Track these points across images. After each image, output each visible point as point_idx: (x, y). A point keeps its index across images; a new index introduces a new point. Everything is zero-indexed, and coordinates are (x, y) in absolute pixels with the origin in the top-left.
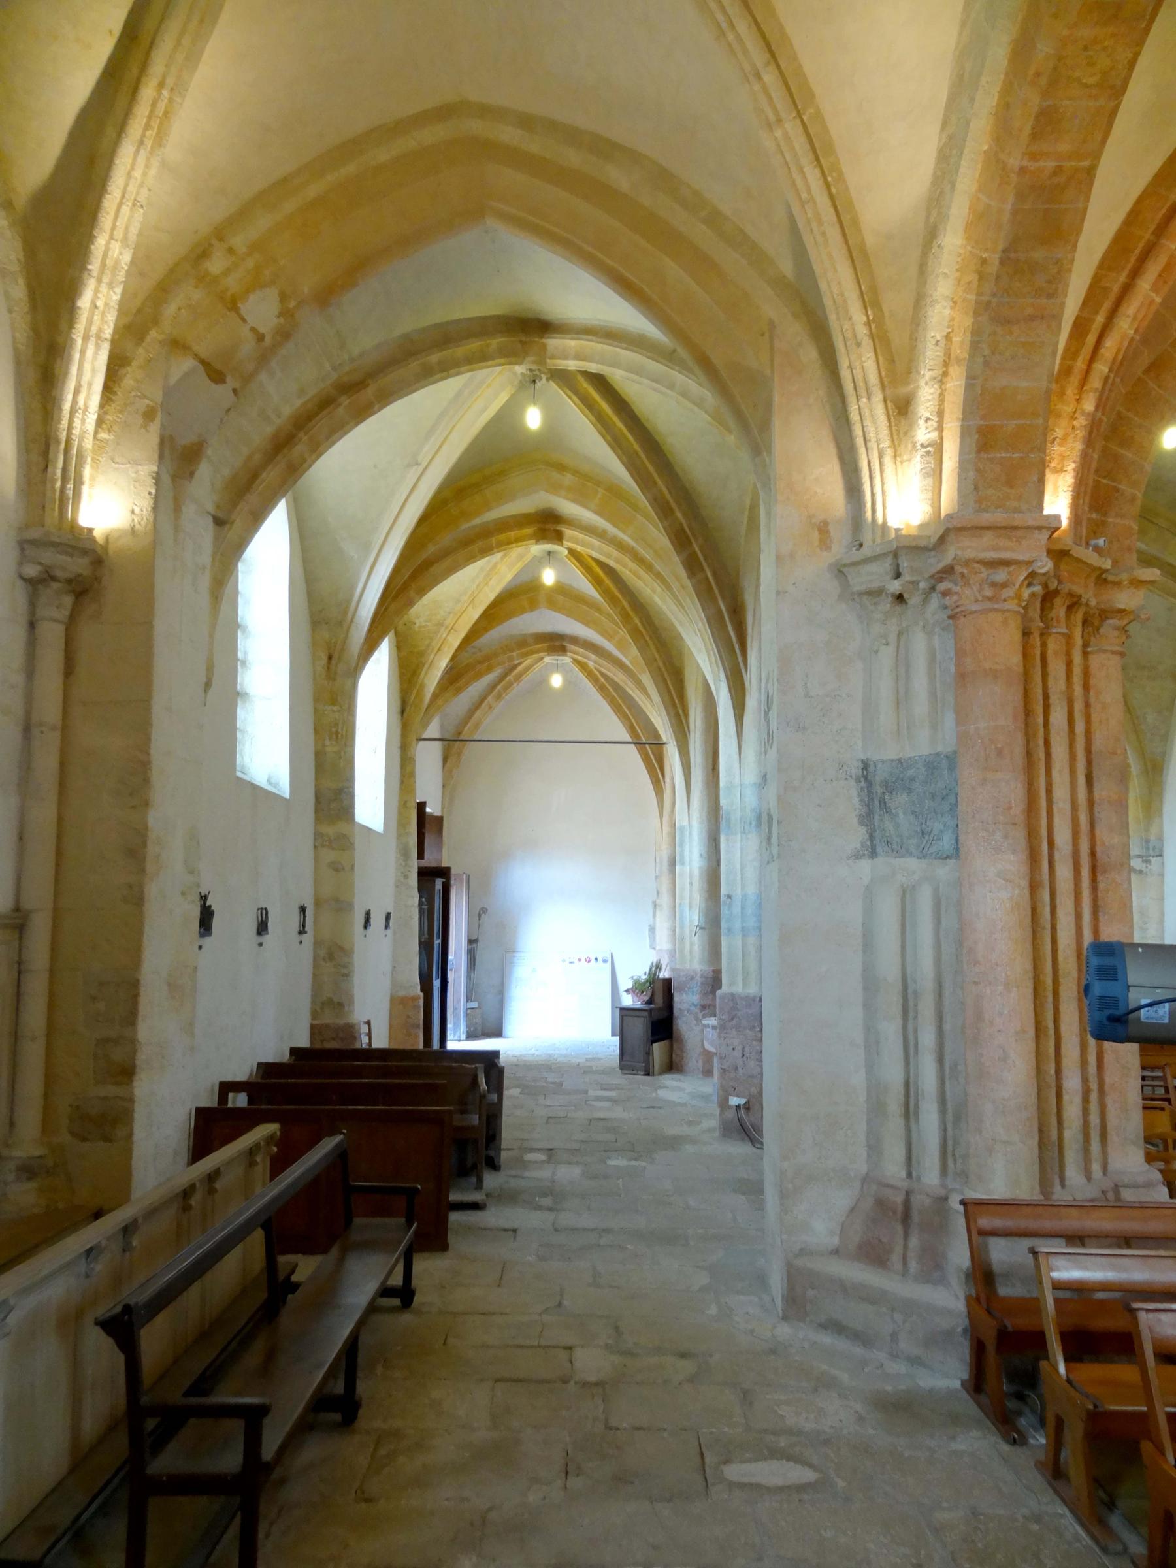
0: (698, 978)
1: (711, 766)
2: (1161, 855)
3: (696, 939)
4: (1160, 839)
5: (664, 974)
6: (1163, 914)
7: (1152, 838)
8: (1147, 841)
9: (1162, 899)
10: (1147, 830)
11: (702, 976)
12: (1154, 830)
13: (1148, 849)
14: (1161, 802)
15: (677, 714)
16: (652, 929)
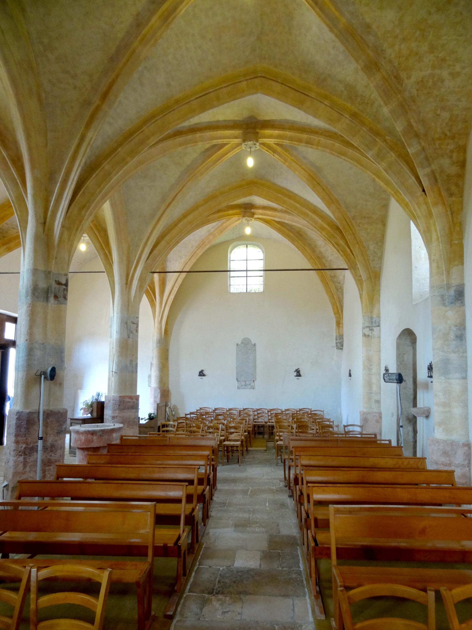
0: (112, 402)
1: (124, 282)
2: (379, 326)
3: (113, 378)
4: (379, 317)
5: (103, 399)
6: (380, 359)
7: (374, 316)
8: (372, 318)
9: (380, 351)
10: (371, 312)
11: (113, 400)
12: (375, 311)
13: (372, 323)
14: (379, 295)
15: (105, 255)
16: (150, 377)
